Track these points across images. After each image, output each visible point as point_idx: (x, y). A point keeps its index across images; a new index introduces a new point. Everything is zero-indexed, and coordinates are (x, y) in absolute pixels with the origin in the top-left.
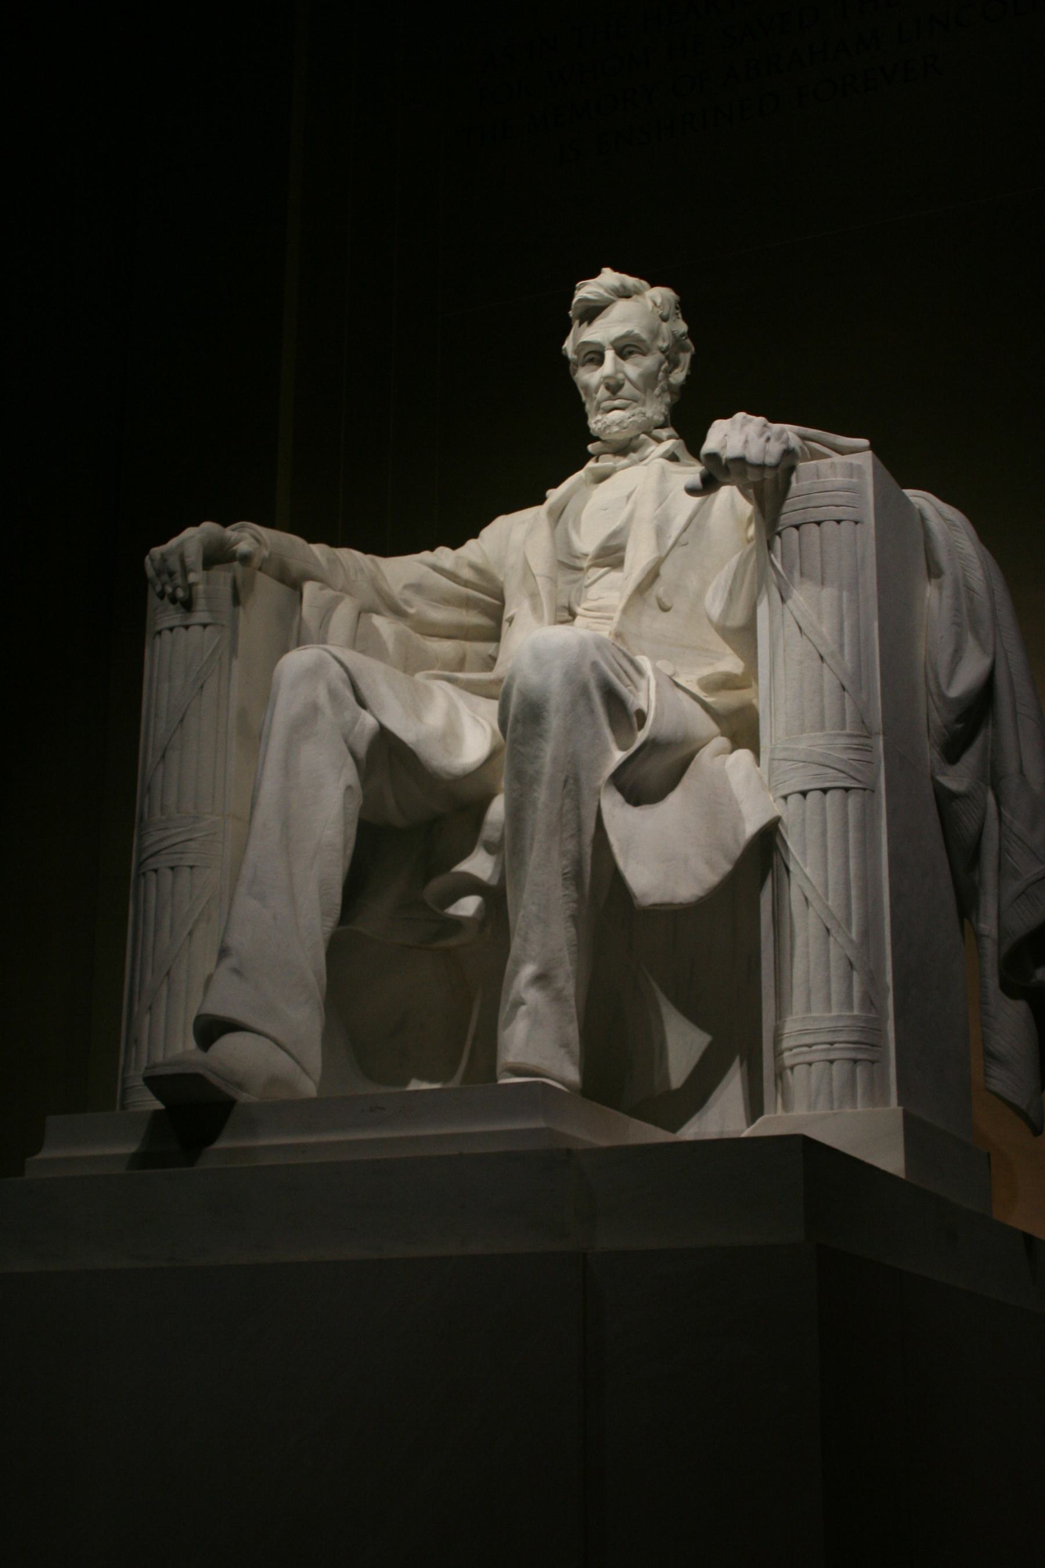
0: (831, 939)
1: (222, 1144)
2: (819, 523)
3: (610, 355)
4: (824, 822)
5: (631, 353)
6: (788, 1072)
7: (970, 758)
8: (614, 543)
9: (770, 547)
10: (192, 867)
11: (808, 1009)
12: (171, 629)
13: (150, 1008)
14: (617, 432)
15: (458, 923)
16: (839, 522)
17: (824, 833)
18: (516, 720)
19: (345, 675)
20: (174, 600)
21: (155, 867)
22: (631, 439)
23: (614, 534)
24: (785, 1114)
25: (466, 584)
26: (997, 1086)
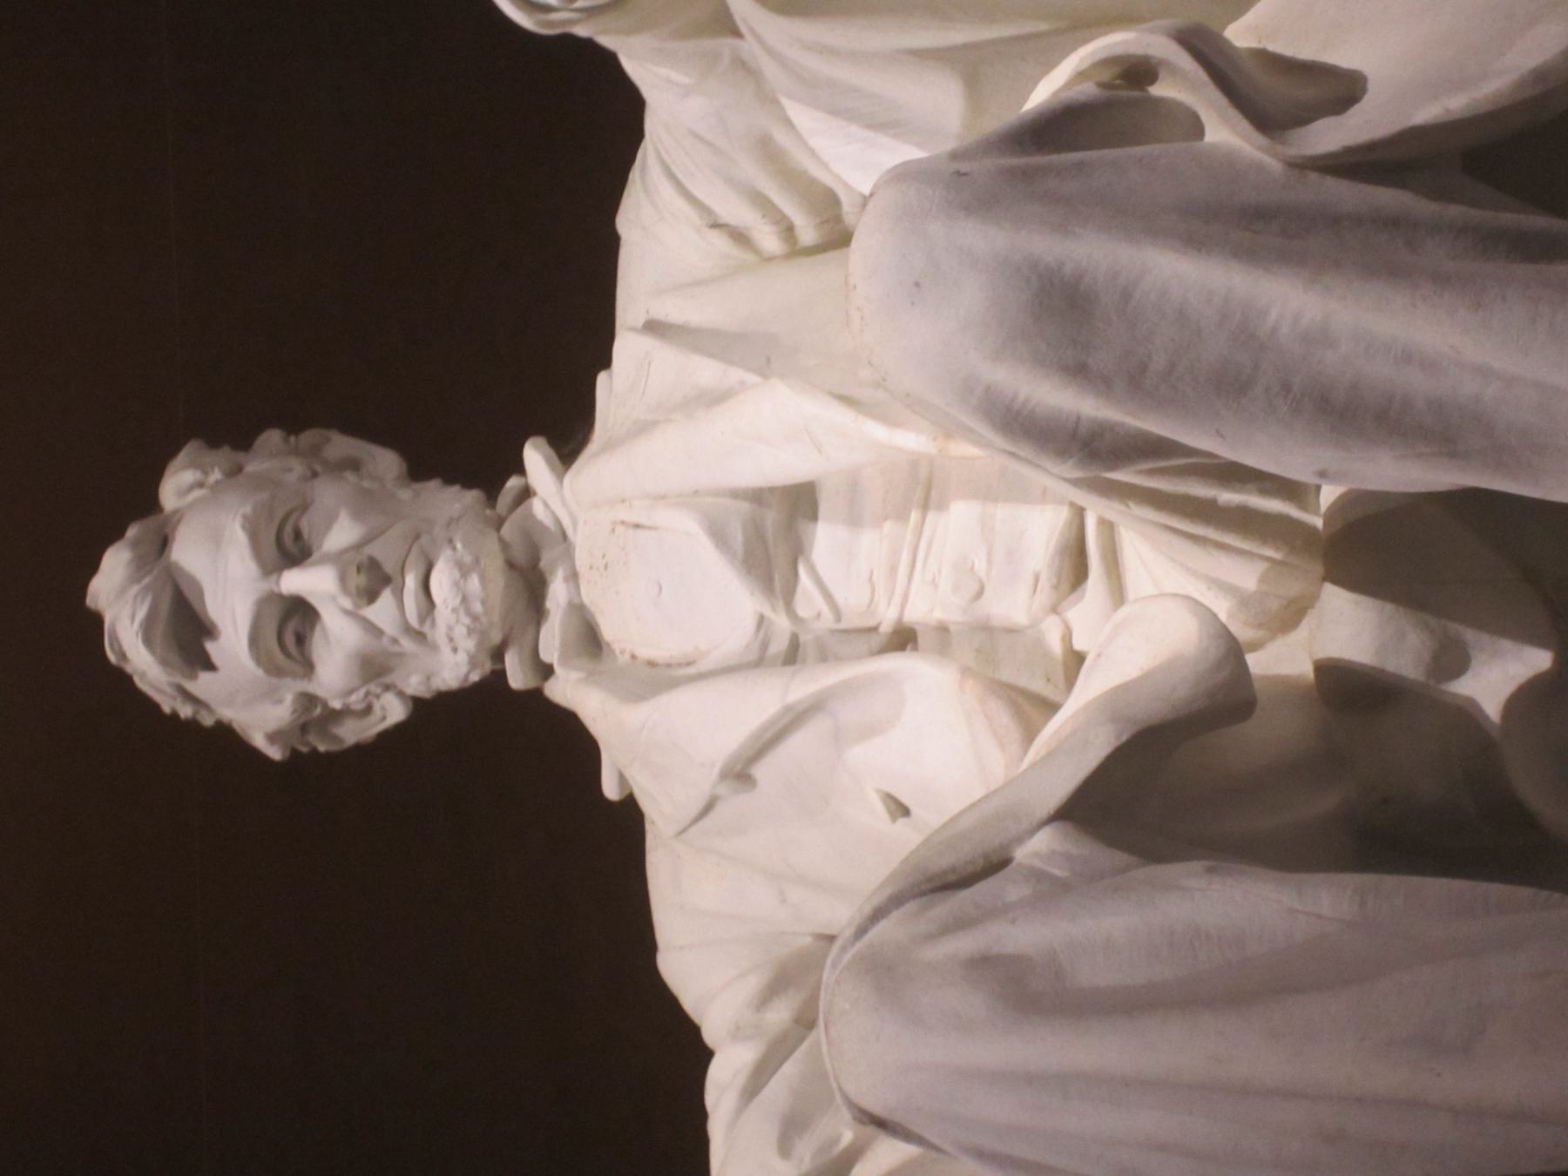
3: (294, 582)
5: (298, 535)
8: (738, 538)
14: (483, 579)
18: (1078, 372)
19: (911, 906)
22: (511, 565)
23: (718, 536)
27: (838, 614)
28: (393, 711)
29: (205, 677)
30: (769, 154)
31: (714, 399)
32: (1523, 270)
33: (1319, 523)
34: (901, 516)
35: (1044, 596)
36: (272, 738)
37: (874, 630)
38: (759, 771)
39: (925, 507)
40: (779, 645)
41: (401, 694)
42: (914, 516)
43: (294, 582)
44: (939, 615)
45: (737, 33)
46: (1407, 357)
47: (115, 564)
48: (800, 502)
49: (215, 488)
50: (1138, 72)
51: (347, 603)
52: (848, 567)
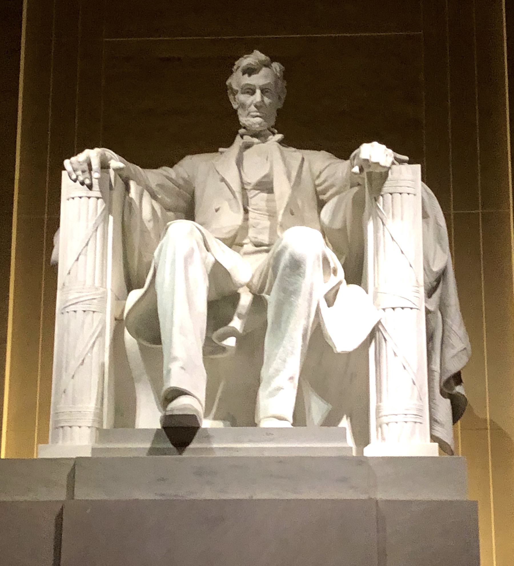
2: (401, 194)
5: (267, 92)
7: (436, 296)
9: (376, 200)
10: (94, 312)
12: (80, 197)
13: (73, 376)
15: (224, 349)
16: (408, 194)
18: (286, 267)
20: (82, 183)
21: (75, 310)
22: (261, 131)
23: (265, 176)
25: (179, 186)
26: (438, 434)
27: (251, 198)
28: (235, 106)
29: (241, 74)
30: (332, 186)
31: (289, 177)
33: (263, 294)
34: (268, 211)
35: (253, 240)
36: (230, 83)
37: (248, 205)
38: (223, 183)
39: (269, 216)
40: (246, 187)
41: (238, 108)
42: (267, 214)
43: (258, 92)
44: (250, 219)
45: (351, 187)
46: (288, 318)
47: (262, 57)
48: (270, 191)
49: (276, 75)
50: (335, 272)
51: (254, 102)
52: (258, 200)
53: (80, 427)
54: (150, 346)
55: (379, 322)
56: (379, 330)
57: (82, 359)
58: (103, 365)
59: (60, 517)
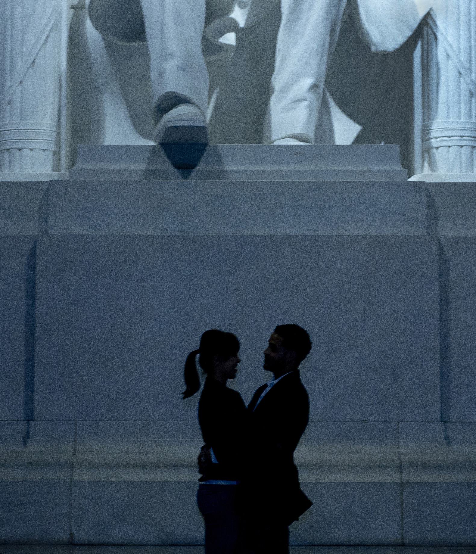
0: (462, 79)
1: (201, 167)
4: (459, 13)
6: (435, 150)
11: (448, 117)
15: (221, 48)
17: (459, 19)
24: (430, 173)
32: (329, 30)
46: (311, 5)
53: (32, 150)
54: (120, 43)
55: (428, 15)
56: (428, 24)
57: (33, 60)
58: (59, 67)
59: (33, 254)
